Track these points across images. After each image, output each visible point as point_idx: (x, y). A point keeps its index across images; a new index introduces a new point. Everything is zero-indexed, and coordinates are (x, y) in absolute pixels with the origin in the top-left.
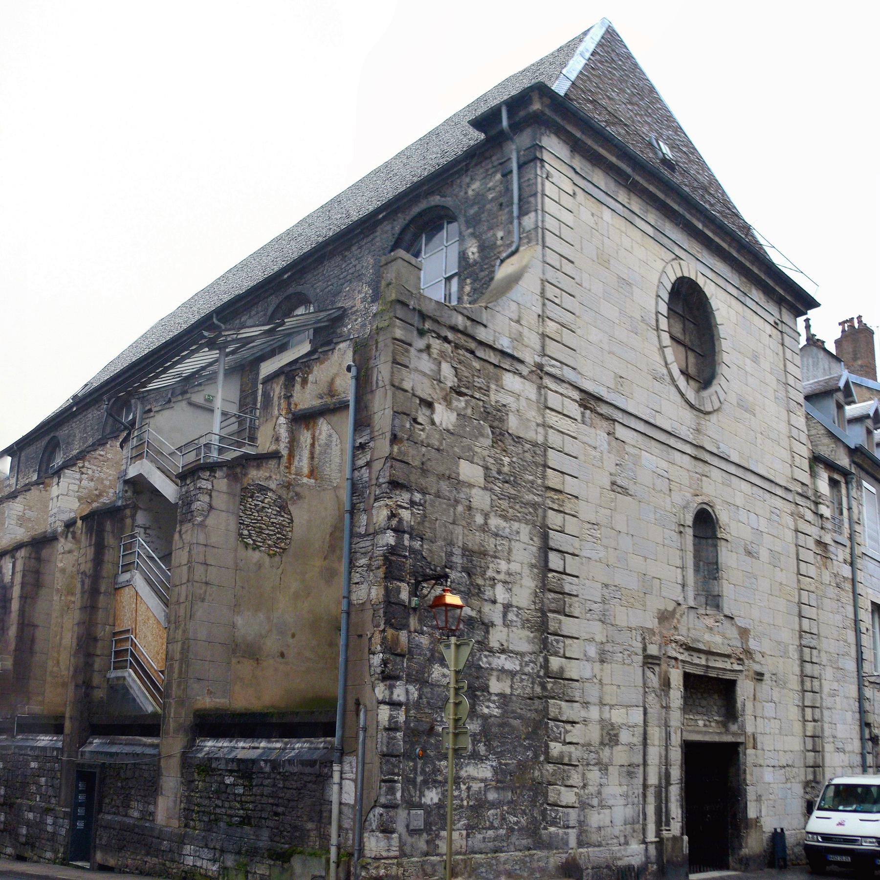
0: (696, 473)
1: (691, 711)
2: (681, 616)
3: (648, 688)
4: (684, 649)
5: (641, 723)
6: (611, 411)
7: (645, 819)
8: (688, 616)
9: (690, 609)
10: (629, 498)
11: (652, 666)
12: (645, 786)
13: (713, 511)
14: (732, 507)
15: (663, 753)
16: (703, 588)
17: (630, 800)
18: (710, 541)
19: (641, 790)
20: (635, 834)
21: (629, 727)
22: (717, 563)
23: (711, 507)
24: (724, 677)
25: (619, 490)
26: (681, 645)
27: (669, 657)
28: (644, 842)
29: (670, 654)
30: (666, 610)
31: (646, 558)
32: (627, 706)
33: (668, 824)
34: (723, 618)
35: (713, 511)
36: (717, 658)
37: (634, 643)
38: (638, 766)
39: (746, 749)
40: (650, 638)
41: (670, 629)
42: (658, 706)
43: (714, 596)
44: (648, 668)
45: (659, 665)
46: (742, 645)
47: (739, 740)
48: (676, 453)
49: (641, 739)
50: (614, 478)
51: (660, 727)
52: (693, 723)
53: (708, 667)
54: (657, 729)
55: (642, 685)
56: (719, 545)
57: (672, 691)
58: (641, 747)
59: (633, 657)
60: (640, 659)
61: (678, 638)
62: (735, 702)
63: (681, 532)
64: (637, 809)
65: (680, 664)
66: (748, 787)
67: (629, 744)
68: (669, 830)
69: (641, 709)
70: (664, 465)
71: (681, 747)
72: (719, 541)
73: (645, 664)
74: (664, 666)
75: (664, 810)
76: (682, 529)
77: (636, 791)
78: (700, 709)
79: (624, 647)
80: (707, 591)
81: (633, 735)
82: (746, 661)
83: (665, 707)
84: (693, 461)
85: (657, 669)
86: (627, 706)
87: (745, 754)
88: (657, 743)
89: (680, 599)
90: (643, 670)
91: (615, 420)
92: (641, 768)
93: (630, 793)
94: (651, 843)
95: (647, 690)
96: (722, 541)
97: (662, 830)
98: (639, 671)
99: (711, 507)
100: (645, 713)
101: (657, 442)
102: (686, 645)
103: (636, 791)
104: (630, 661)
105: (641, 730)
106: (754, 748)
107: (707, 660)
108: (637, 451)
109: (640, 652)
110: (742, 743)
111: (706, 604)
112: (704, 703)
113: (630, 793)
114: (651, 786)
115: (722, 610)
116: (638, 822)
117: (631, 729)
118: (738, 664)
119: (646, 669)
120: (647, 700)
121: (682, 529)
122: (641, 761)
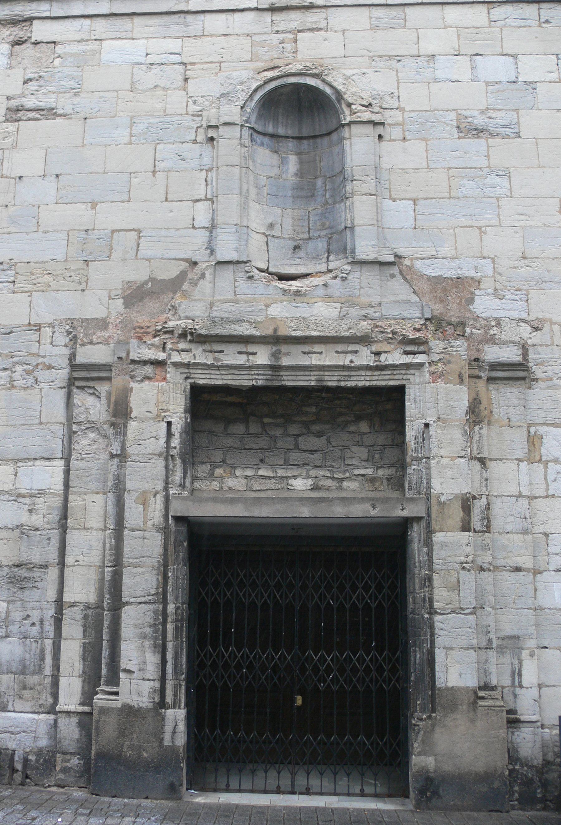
0: (277, 32)
1: (262, 461)
2: (194, 283)
3: (79, 423)
4: (191, 341)
5: (59, 487)
6: (21, 8)
7: (56, 666)
8: (214, 282)
9: (218, 267)
10: (59, 120)
11: (91, 384)
12: (60, 604)
13: (324, 81)
14: (410, 63)
15: (111, 542)
16: (323, 225)
17: (14, 629)
18: (334, 136)
19: (52, 612)
20: (27, 694)
21: (20, 496)
22: (342, 171)
23: (315, 76)
24: (349, 384)
25: (31, 115)
26: (183, 335)
27: (133, 362)
28: (52, 710)
29: (134, 356)
30: (152, 279)
31: (94, 205)
32: (15, 461)
33: (114, 680)
34: (348, 267)
35: (324, 81)
36: (317, 348)
37: (46, 349)
38: (45, 566)
39: (430, 532)
40: (86, 335)
41: (162, 312)
42: (104, 456)
43: (341, 232)
44: (78, 387)
45: (109, 379)
46: (422, 313)
47: (405, 514)
48: (208, 16)
49: (55, 516)
50: (14, 103)
51: (105, 494)
52: (270, 484)
53: (276, 368)
54: (99, 498)
55: (63, 419)
56: (346, 135)
57: (132, 426)
58: (56, 532)
59: (42, 375)
60: (64, 373)
61: (171, 324)
62: (403, 433)
63: (212, 139)
64: (35, 647)
65: (172, 373)
66: (437, 618)
67: (19, 527)
68: (117, 694)
69: (62, 463)
70: (173, 45)
71: (164, 530)
72: (346, 129)
73: (71, 382)
74: (118, 381)
75: (105, 653)
76: (211, 133)
77: (35, 615)
78: (295, 456)
79: (16, 359)
80: (330, 228)
81: (30, 511)
82: (437, 345)
83: (117, 456)
84: (268, 17)
85: (103, 388)
86: (15, 461)
87: (428, 542)
88: (96, 522)
89: (201, 256)
90: (69, 397)
91: (31, 19)
92: (53, 573)
93: (17, 616)
94: (68, 713)
95: (75, 428)
96: (353, 126)
97: (97, 693)
98: (60, 397)
99: (315, 76)
100: (67, 472)
101: (148, 17)
102: (192, 334)
103: (35, 615)
104: (31, 381)
105: (58, 501)
106: (466, 527)
107: (276, 355)
108: (93, 45)
109: (65, 363)
110: (419, 519)
111: (329, 252)
112: (312, 442)
113: (17, 616)
114: (72, 605)
115: (353, 251)
116: (40, 670)
117: (27, 500)
118: (406, 353)
119: (75, 390)
120: (75, 446)
121: (211, 133)
122: (53, 557)
